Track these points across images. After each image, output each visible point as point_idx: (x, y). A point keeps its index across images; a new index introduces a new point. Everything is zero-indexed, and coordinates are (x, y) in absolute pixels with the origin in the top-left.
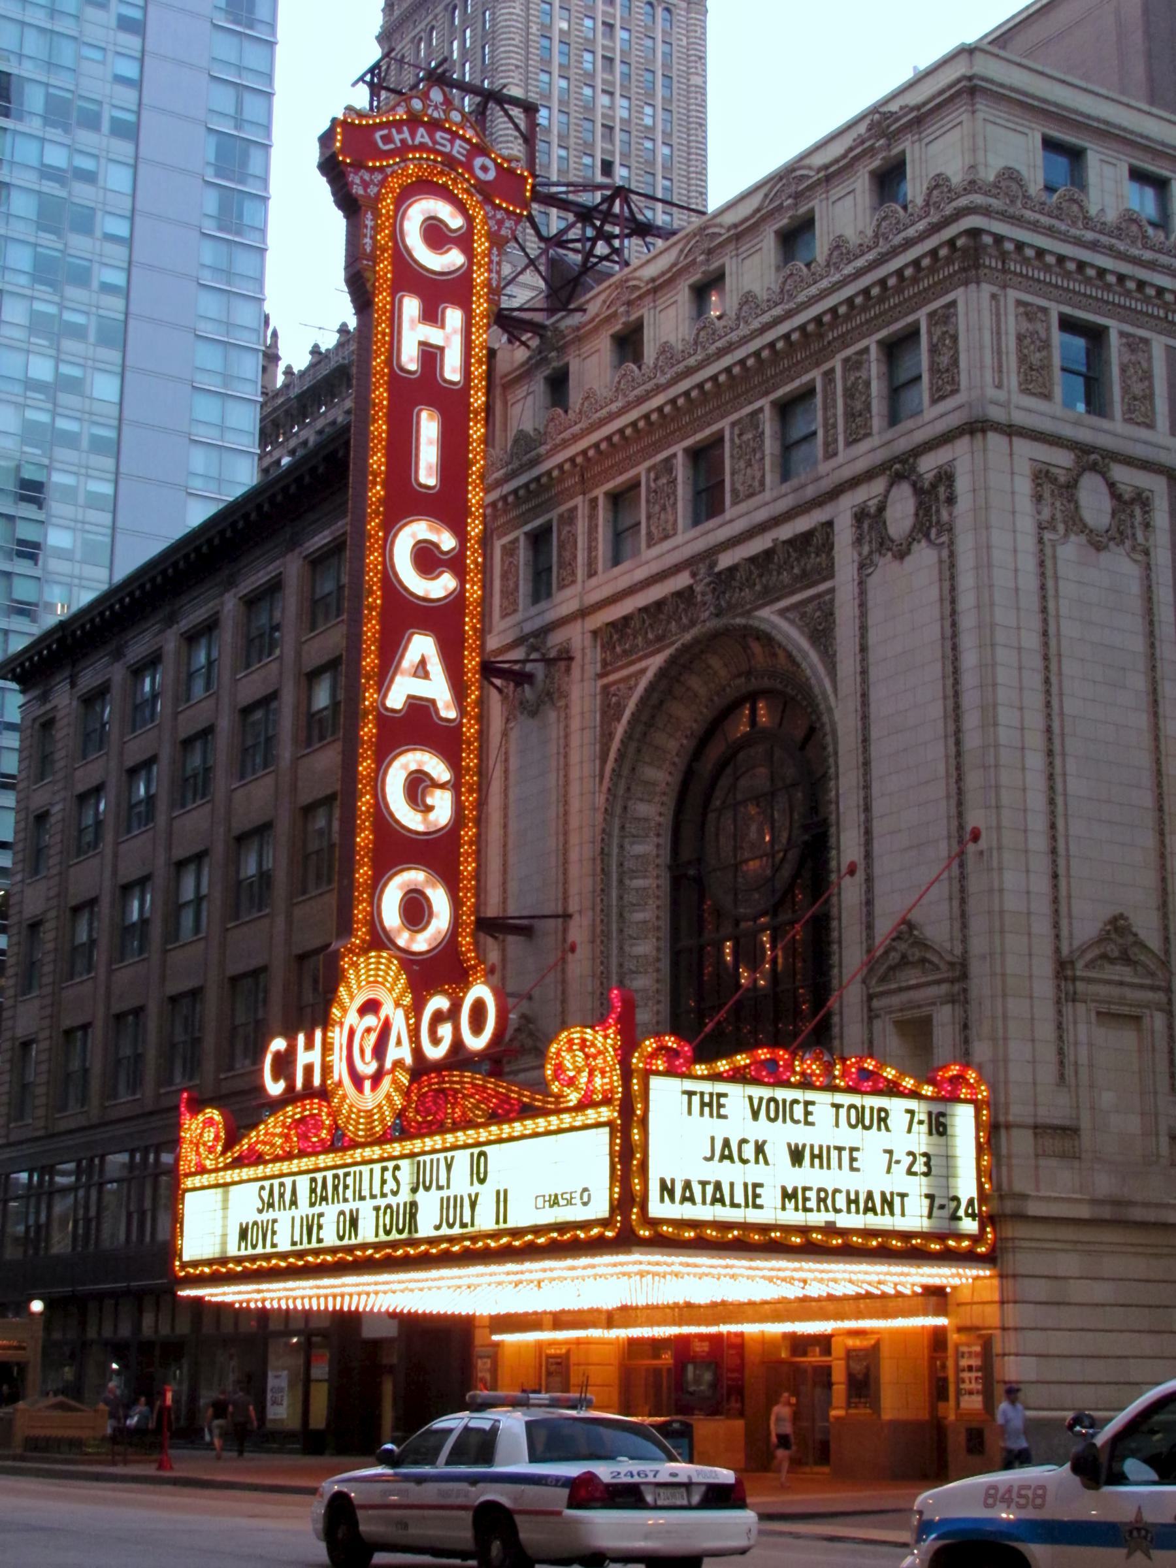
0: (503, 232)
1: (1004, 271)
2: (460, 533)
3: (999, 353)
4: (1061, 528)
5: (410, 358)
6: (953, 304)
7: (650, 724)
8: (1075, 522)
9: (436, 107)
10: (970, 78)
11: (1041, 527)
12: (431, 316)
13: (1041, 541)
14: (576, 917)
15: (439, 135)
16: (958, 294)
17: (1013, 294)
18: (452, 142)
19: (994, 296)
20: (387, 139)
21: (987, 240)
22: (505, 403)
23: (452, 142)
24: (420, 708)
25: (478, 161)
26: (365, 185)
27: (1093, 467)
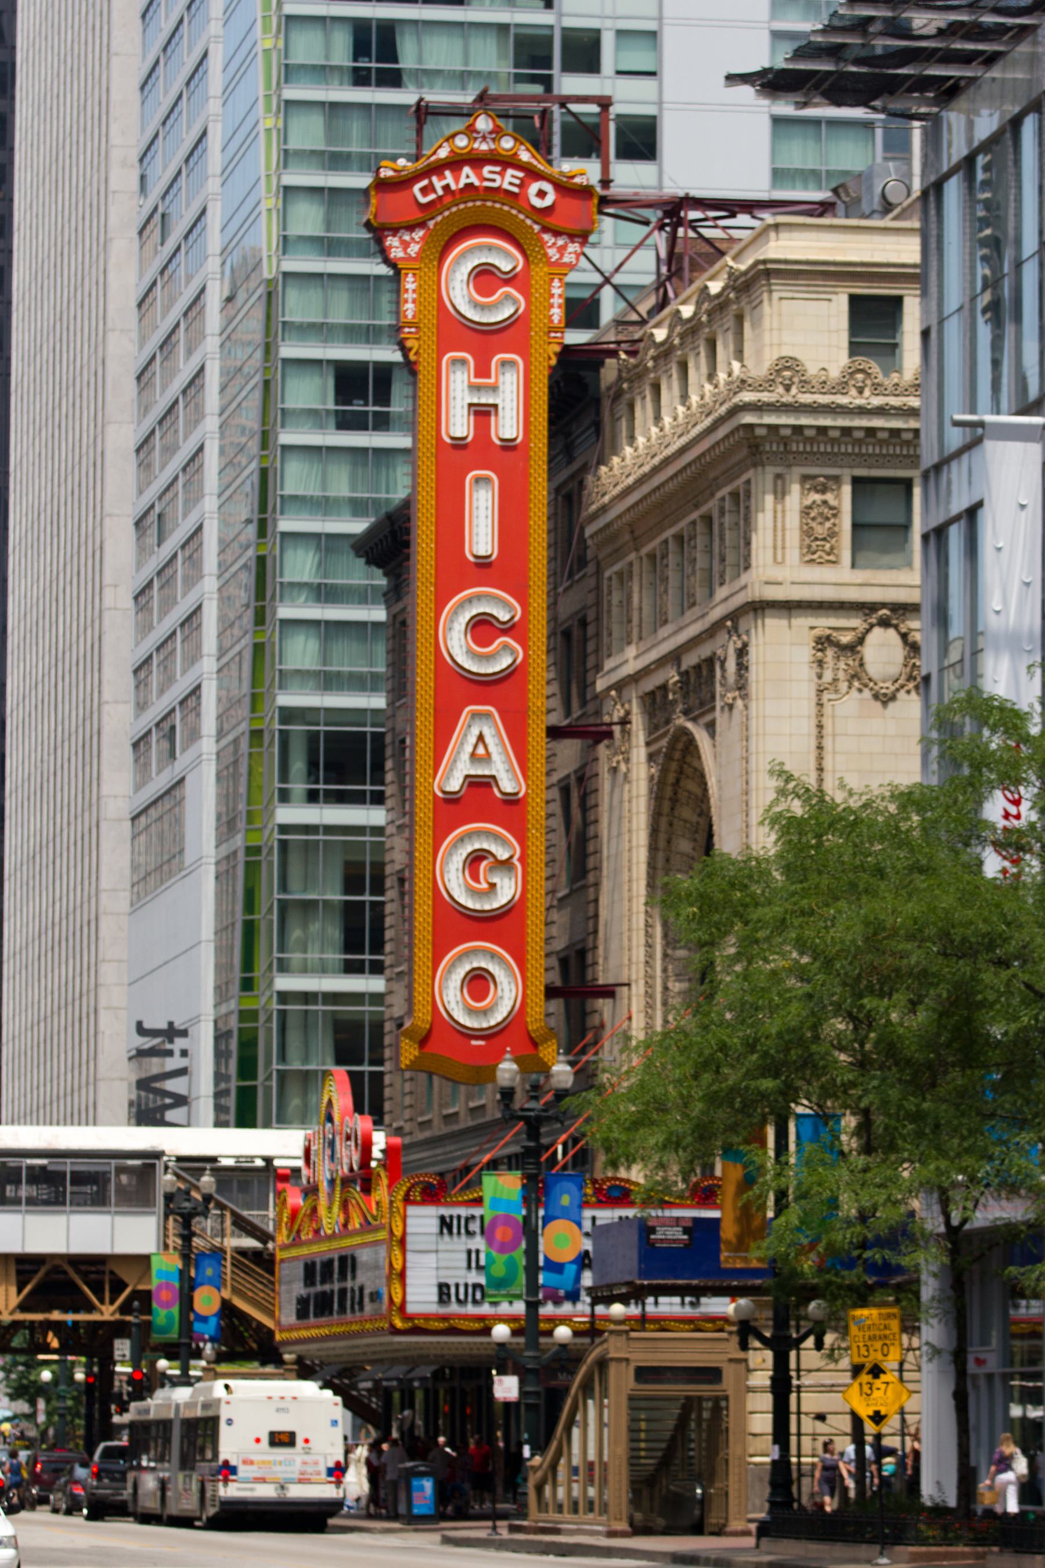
0: (566, 259)
1: (787, 452)
2: (522, 596)
3: (784, 529)
4: (843, 686)
5: (459, 425)
6: (748, 482)
7: (674, 801)
8: (858, 676)
9: (484, 138)
10: (765, 262)
11: (820, 691)
12: (482, 371)
13: (820, 705)
14: (634, 987)
15: (486, 170)
16: (750, 474)
17: (798, 471)
18: (502, 174)
19: (778, 476)
20: (424, 191)
21: (760, 432)
22: (612, 414)
23: (502, 174)
24: (480, 785)
25: (534, 188)
26: (405, 245)
27: (884, 623)
